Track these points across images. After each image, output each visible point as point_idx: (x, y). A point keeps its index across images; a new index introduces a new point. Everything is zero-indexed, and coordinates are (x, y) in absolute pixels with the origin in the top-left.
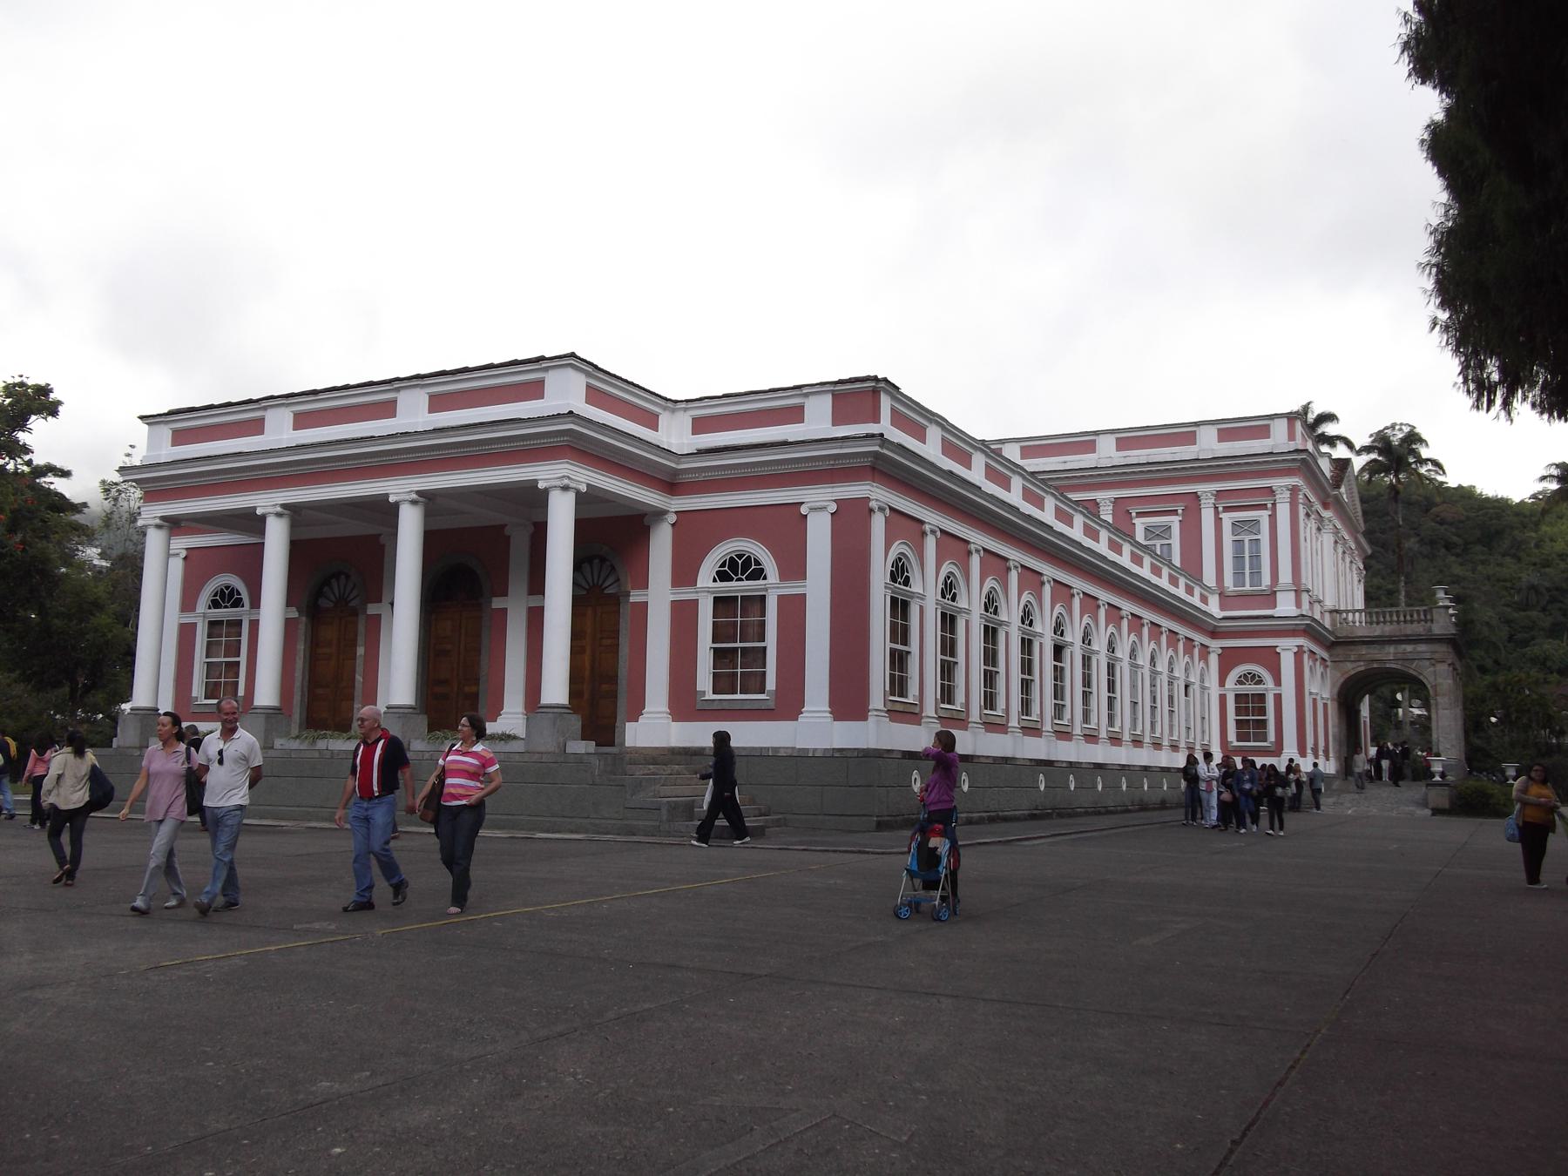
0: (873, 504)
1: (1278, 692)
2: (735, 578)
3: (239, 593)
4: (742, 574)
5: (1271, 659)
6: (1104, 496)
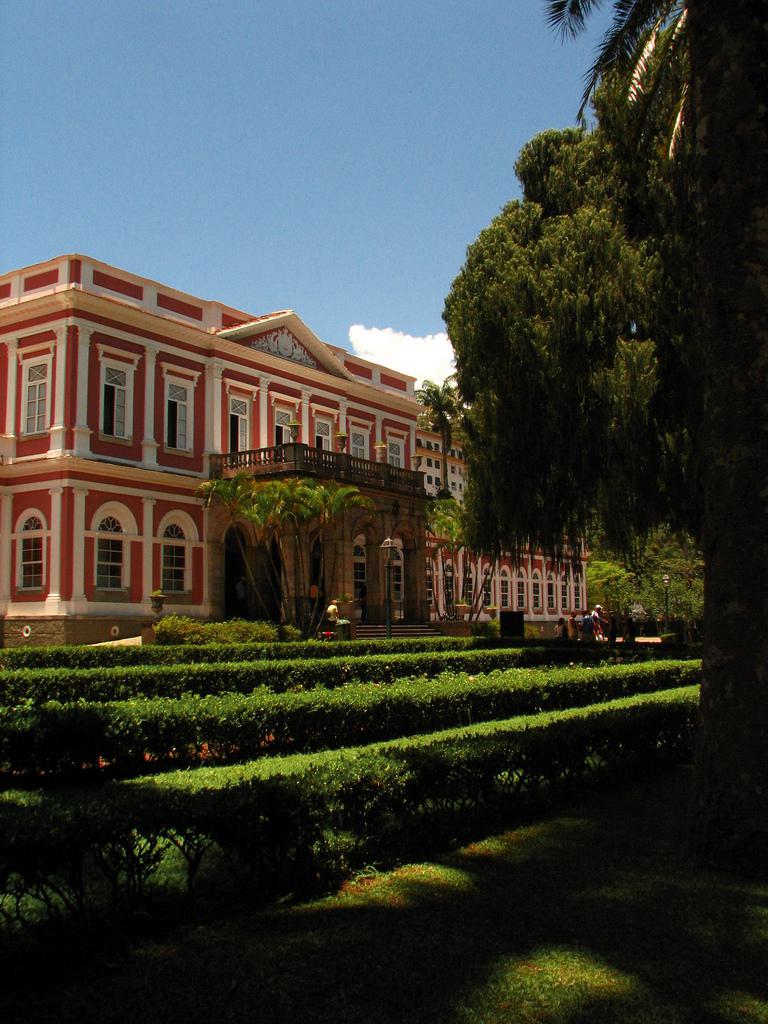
5: (42, 500)
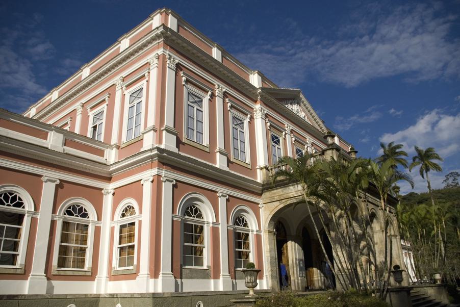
1: (140, 219)
2: (6, 204)
4: (7, 202)
5: (135, 190)
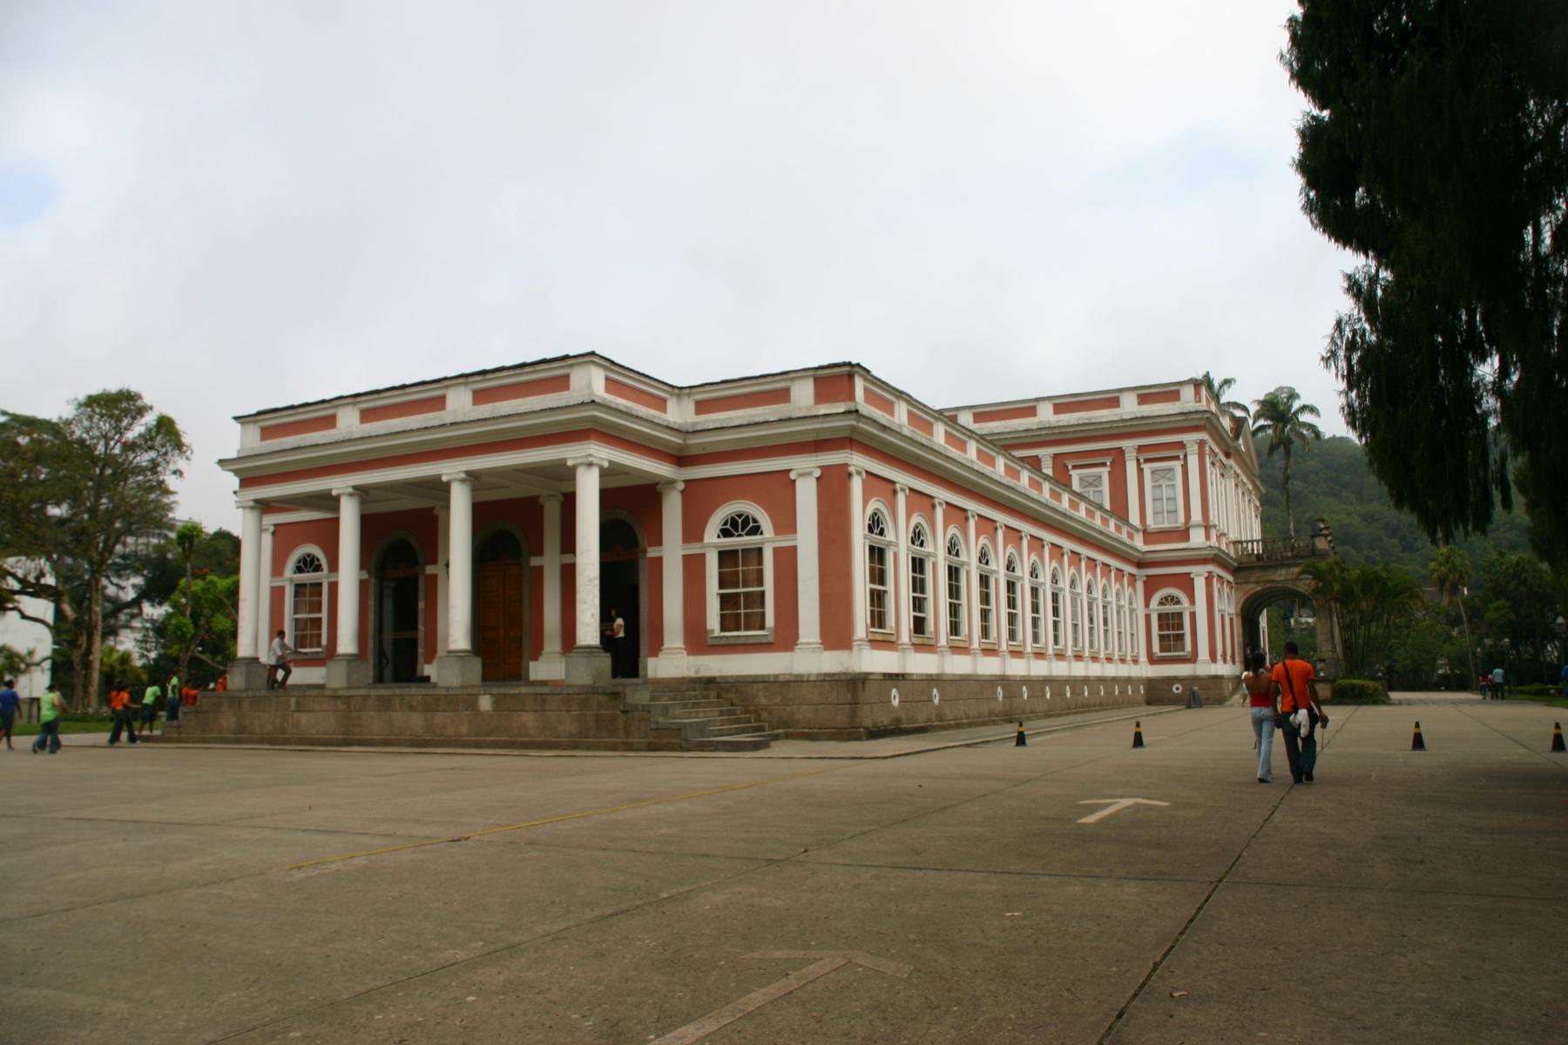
0: (852, 469)
1: (1192, 610)
3: (318, 560)
5: (1186, 583)
6: (1045, 453)
